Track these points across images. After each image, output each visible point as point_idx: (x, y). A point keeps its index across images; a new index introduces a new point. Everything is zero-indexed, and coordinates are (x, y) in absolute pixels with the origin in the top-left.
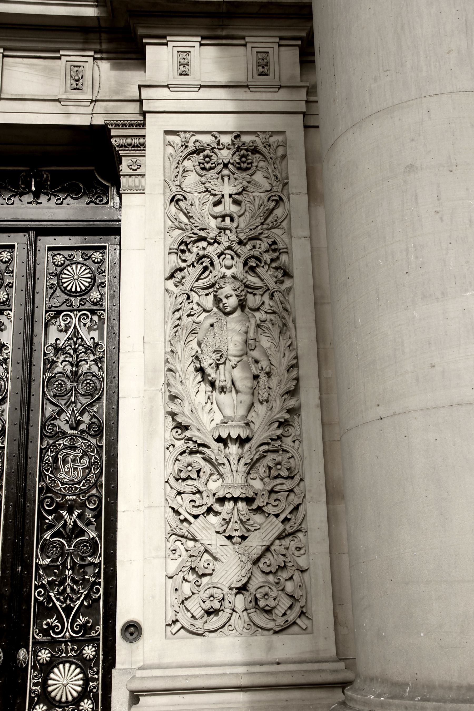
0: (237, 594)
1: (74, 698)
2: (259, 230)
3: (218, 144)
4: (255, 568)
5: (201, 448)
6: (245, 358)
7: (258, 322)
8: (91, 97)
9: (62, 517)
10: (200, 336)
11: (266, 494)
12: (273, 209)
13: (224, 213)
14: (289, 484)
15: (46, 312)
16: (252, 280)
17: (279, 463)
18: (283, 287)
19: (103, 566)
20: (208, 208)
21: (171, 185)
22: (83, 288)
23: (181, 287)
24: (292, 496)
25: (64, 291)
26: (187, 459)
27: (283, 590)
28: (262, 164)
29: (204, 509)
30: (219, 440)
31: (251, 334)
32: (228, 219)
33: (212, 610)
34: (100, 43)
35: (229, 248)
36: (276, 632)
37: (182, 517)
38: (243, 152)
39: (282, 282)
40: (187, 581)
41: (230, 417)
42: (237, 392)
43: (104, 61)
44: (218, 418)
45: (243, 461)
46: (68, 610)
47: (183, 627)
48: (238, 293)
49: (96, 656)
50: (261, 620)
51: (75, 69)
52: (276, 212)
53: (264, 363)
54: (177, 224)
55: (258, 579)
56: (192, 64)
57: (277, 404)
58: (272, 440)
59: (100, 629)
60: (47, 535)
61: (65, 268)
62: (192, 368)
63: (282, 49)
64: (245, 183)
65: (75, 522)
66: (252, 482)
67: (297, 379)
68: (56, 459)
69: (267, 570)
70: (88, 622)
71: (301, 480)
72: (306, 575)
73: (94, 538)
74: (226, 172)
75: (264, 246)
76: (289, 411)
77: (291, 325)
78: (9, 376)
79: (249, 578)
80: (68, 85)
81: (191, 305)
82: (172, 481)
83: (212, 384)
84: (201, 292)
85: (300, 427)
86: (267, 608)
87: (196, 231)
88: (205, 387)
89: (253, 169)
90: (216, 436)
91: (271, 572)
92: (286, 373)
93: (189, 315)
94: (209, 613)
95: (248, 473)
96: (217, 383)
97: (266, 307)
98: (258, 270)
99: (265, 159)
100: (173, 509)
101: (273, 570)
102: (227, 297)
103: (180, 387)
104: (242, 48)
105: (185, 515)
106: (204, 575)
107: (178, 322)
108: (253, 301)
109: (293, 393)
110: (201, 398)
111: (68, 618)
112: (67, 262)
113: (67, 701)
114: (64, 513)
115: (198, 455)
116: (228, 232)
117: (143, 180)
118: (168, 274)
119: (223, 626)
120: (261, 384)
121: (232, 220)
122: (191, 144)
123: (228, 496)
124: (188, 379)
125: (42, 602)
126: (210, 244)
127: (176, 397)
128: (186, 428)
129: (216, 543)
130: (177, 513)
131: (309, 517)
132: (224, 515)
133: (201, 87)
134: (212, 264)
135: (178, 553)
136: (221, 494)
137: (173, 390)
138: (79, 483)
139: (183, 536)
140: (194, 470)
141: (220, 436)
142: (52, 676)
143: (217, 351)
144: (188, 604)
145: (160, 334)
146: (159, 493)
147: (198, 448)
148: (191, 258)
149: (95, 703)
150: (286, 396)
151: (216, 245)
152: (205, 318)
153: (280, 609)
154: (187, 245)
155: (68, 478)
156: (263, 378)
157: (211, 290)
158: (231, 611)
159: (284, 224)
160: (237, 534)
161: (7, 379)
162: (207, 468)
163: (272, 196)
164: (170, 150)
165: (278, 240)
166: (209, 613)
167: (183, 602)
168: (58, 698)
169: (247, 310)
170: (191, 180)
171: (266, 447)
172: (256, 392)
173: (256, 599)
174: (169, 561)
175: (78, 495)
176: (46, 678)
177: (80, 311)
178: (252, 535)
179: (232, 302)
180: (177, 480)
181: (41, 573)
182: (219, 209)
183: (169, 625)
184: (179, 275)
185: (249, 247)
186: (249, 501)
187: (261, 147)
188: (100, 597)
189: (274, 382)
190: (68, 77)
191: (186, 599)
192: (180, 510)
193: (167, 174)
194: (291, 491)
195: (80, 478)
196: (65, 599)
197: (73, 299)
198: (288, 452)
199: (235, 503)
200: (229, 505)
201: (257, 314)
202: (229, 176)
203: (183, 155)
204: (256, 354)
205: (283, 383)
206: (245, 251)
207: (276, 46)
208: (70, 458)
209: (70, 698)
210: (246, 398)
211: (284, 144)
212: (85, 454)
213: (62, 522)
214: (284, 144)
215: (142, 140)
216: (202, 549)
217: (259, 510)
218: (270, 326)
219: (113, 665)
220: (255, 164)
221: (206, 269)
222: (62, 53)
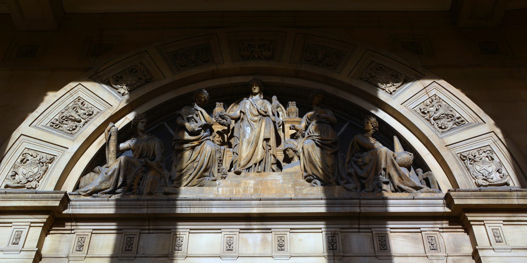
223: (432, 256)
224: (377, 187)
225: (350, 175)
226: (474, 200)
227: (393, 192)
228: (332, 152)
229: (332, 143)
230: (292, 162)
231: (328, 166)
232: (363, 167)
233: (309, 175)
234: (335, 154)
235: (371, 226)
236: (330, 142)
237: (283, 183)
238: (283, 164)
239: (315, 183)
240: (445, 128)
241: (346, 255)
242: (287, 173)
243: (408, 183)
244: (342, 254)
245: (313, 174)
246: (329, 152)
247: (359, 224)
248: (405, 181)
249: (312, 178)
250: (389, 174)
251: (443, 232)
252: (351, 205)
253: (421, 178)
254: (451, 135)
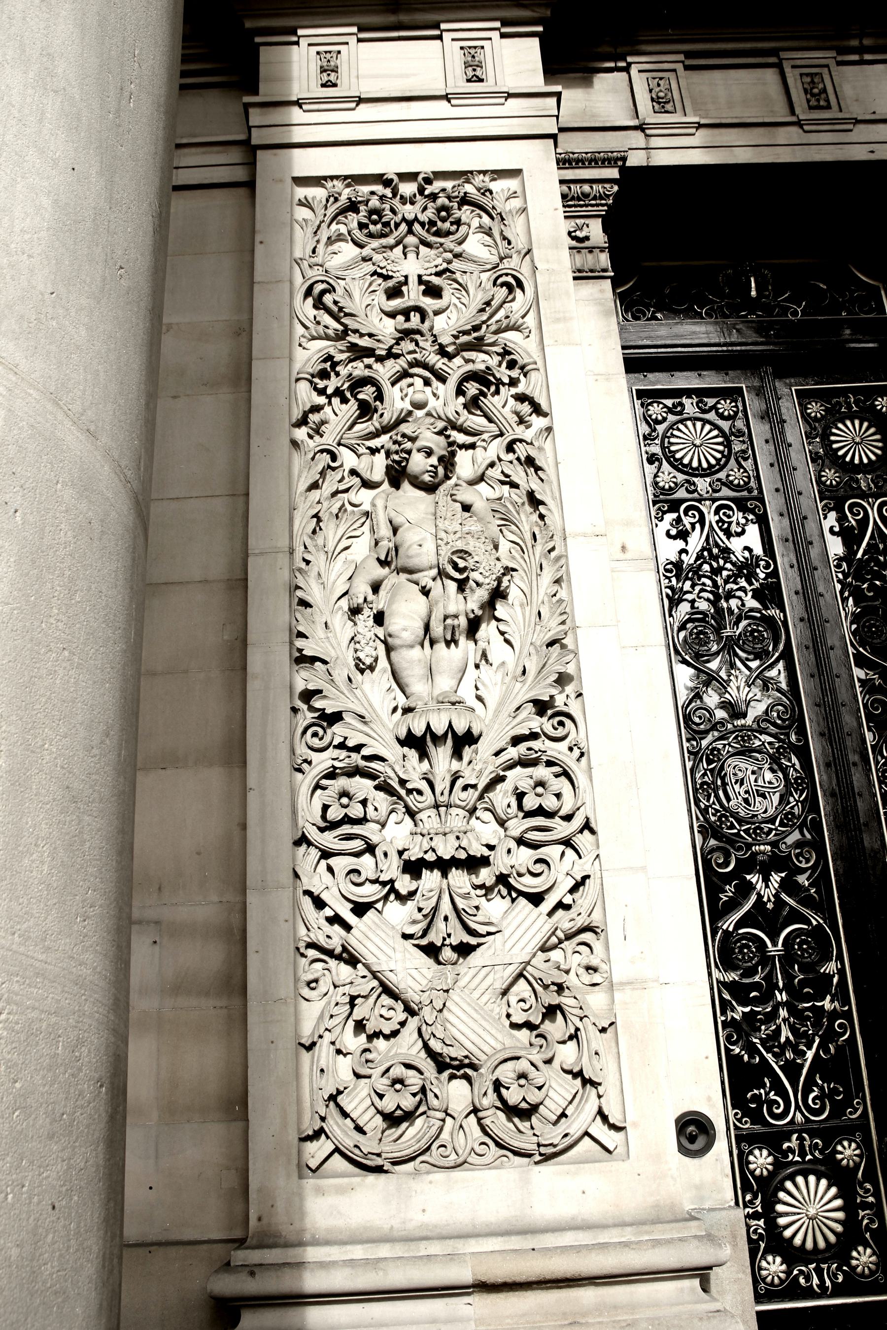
32: (415, 318)
33: (399, 1112)
47: (337, 1150)
94: (393, 1120)
123: (430, 857)
133: (360, 101)
136: (414, 854)
153: (552, 1106)
158: (441, 1115)
162: (381, 800)
163: (501, 276)
166: (393, 1120)
182: (396, 303)
199: (445, 875)
200: (431, 879)
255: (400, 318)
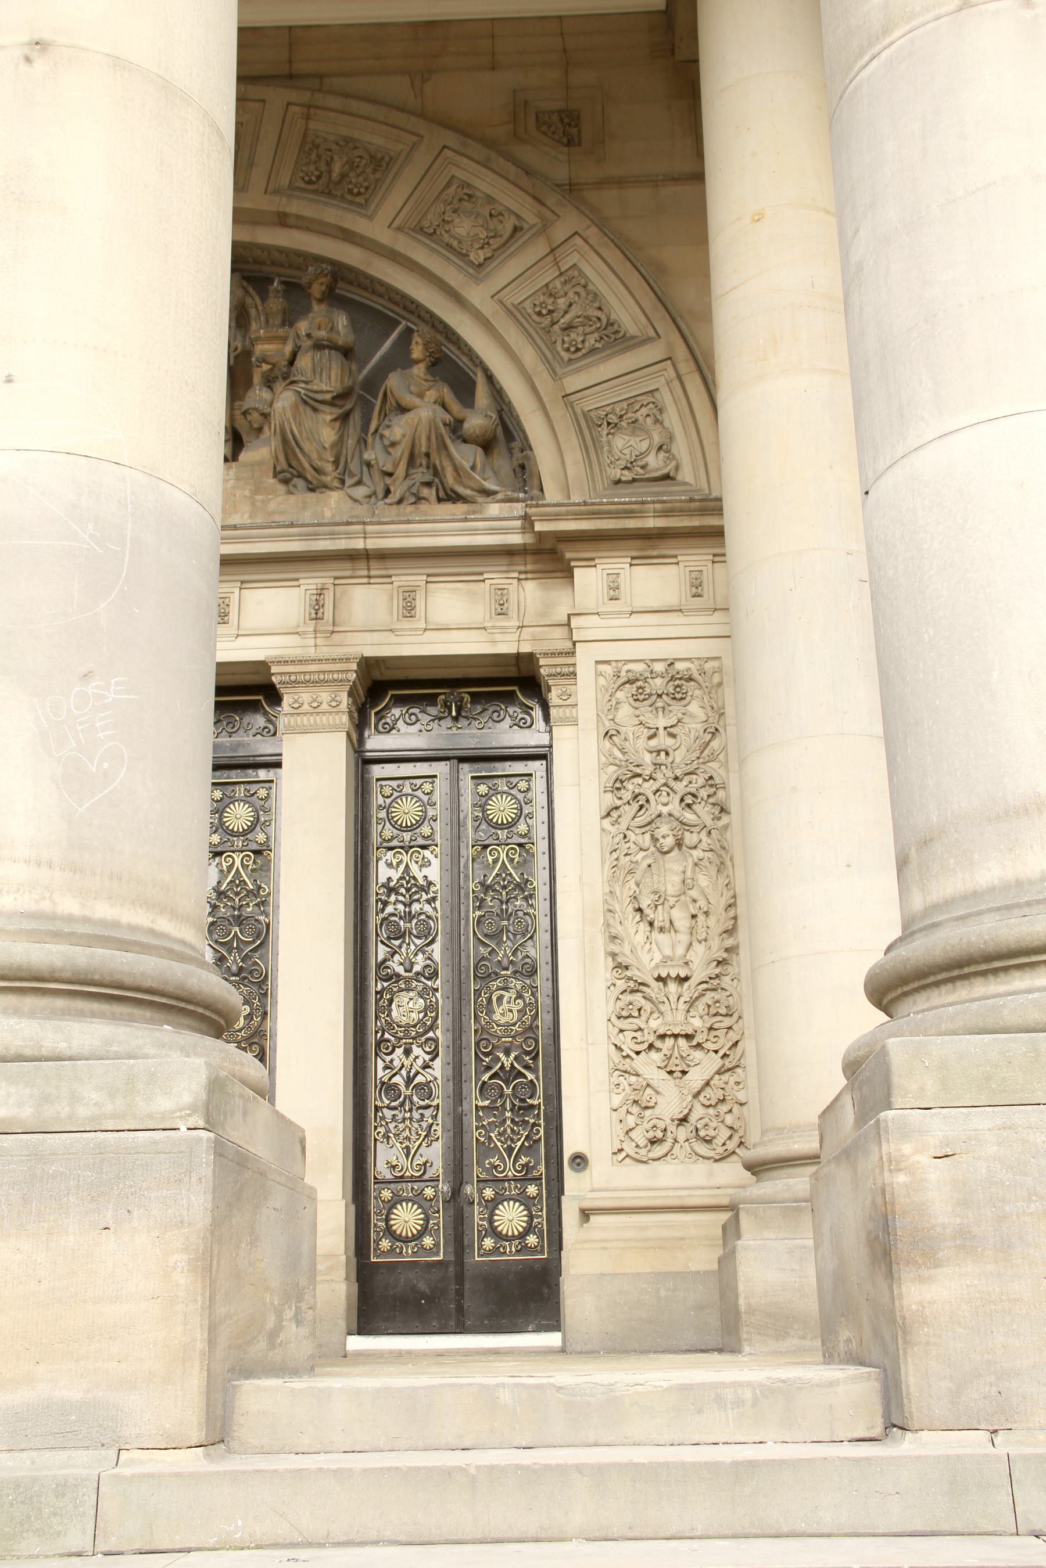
0: (678, 1125)
1: (520, 1233)
2: (695, 765)
3: (652, 672)
4: (695, 1102)
5: (641, 987)
6: (683, 898)
7: (696, 860)
8: (517, 624)
9: (499, 1059)
10: (638, 876)
11: (706, 1031)
12: (710, 741)
13: (659, 748)
14: (727, 1022)
15: (473, 846)
16: (689, 816)
17: (718, 1002)
18: (720, 824)
19: (542, 1108)
20: (642, 743)
21: (604, 718)
22: (510, 820)
23: (617, 826)
24: (731, 1032)
25: (490, 823)
26: (628, 998)
27: (722, 1122)
28: (697, 692)
29: (646, 1045)
30: (659, 979)
31: (689, 874)
34: (525, 565)
35: (665, 785)
36: (716, 1161)
37: (624, 1054)
38: (677, 682)
39: (719, 819)
40: (631, 1113)
41: (669, 957)
42: (676, 931)
43: (529, 582)
44: (658, 958)
45: (682, 1000)
46: (510, 1150)
48: (675, 832)
49: (540, 1194)
50: (702, 1149)
51: (500, 592)
52: (712, 744)
53: (702, 903)
54: (611, 760)
55: (698, 1111)
56: (622, 587)
57: (715, 943)
58: (711, 978)
59: (543, 1169)
60: (486, 1077)
61: (490, 799)
62: (630, 908)
63: (717, 565)
64: (680, 715)
65: (512, 1064)
66: (691, 1020)
67: (735, 918)
68: (489, 1000)
69: (708, 1103)
70: (530, 1162)
71: (740, 1017)
72: (745, 1108)
73: (532, 1081)
74: (660, 704)
75: (701, 781)
76: (727, 950)
77: (728, 863)
78: (439, 915)
79: (690, 1110)
80: (493, 610)
81: (628, 845)
82: (614, 1019)
83: (651, 924)
84: (638, 831)
85: (739, 965)
86: (707, 1138)
87: (631, 768)
88: (644, 927)
89: (688, 699)
90: (656, 976)
91: (710, 1105)
92: (723, 913)
93: (626, 855)
94: (653, 1142)
95: (688, 1011)
96: (656, 924)
97: (703, 845)
98: (694, 807)
99: (700, 687)
100: (616, 1046)
101: (713, 1104)
102: (664, 837)
103: (620, 928)
104: (675, 566)
105: (627, 1051)
106: (646, 1108)
107: (615, 863)
108: (690, 839)
109: (730, 932)
110: (640, 938)
111: (510, 1158)
112: (492, 792)
113: (513, 1236)
114: (501, 1055)
115: (639, 994)
116: (663, 767)
117: (574, 710)
118: (604, 814)
119: (666, 1155)
120: (700, 923)
121: (667, 754)
122: (623, 674)
123: (668, 1033)
124: (627, 919)
125: (484, 1143)
126: (645, 780)
127: (615, 937)
128: (627, 968)
129: (657, 1077)
130: (619, 1048)
131: (747, 1053)
132: (665, 1051)
134: (648, 801)
135: (621, 1087)
136: (661, 1031)
137: (612, 930)
138: (514, 1025)
139: (625, 1072)
140: (636, 1008)
141: (659, 976)
142: (500, 1207)
143: (655, 893)
144: (632, 1134)
145: (597, 874)
146: (601, 1031)
147: (638, 987)
148: (627, 796)
149: (540, 1237)
150: (724, 935)
151: (651, 781)
152: (643, 858)
154: (622, 782)
155: (503, 1021)
156: (701, 918)
157: (647, 828)
159: (721, 757)
160: (679, 1068)
161: (437, 918)
162: (648, 1006)
164: (602, 681)
165: (715, 775)
166: (653, 1142)
167: (627, 1133)
168: (504, 1232)
169: (684, 848)
170: (625, 712)
171: (704, 986)
172: (694, 932)
173: (697, 1130)
174: (613, 1095)
175: (513, 1037)
176: (492, 1214)
177: (507, 845)
178: (692, 1071)
179: (669, 841)
180: (619, 1018)
181: (481, 1114)
183: (614, 1153)
184: (615, 814)
185: (685, 783)
186: (688, 1037)
187: (696, 675)
188: (540, 1138)
189: (712, 921)
190: (493, 602)
191: (631, 1130)
192: (623, 1047)
193: (600, 708)
194: (730, 1028)
195: (515, 1020)
196: (506, 1140)
197: (499, 832)
198: (726, 990)
200: (669, 1042)
201: (695, 853)
202: (664, 708)
203: (616, 686)
204: (694, 893)
205: (721, 922)
206: (680, 787)
207: (710, 564)
208: (505, 1000)
209: (516, 1233)
210: (684, 938)
211: (720, 670)
212: (520, 996)
213: (500, 1064)
214: (720, 670)
215: (571, 669)
216: (645, 1083)
217: (699, 1046)
218: (708, 864)
219: (561, 1191)
220: (690, 694)
221: (641, 807)
222: (486, 576)
223: (494, 627)
224: (407, 494)
225: (369, 465)
226: (573, 522)
227: (440, 500)
228: (334, 416)
229: (334, 398)
230: (262, 437)
231: (325, 448)
232: (390, 450)
233: (284, 471)
234: (344, 418)
235: (391, 572)
236: (328, 397)
237: (234, 488)
238: (245, 438)
239: (295, 486)
240: (578, 350)
241: (336, 629)
242: (245, 465)
243: (472, 484)
244: (331, 628)
245: (290, 466)
246: (329, 418)
247: (369, 569)
248: (464, 480)
249: (288, 476)
250: (435, 467)
251: (526, 579)
252: (349, 536)
253: (516, 463)
254: (579, 370)
255: (655, 754)
